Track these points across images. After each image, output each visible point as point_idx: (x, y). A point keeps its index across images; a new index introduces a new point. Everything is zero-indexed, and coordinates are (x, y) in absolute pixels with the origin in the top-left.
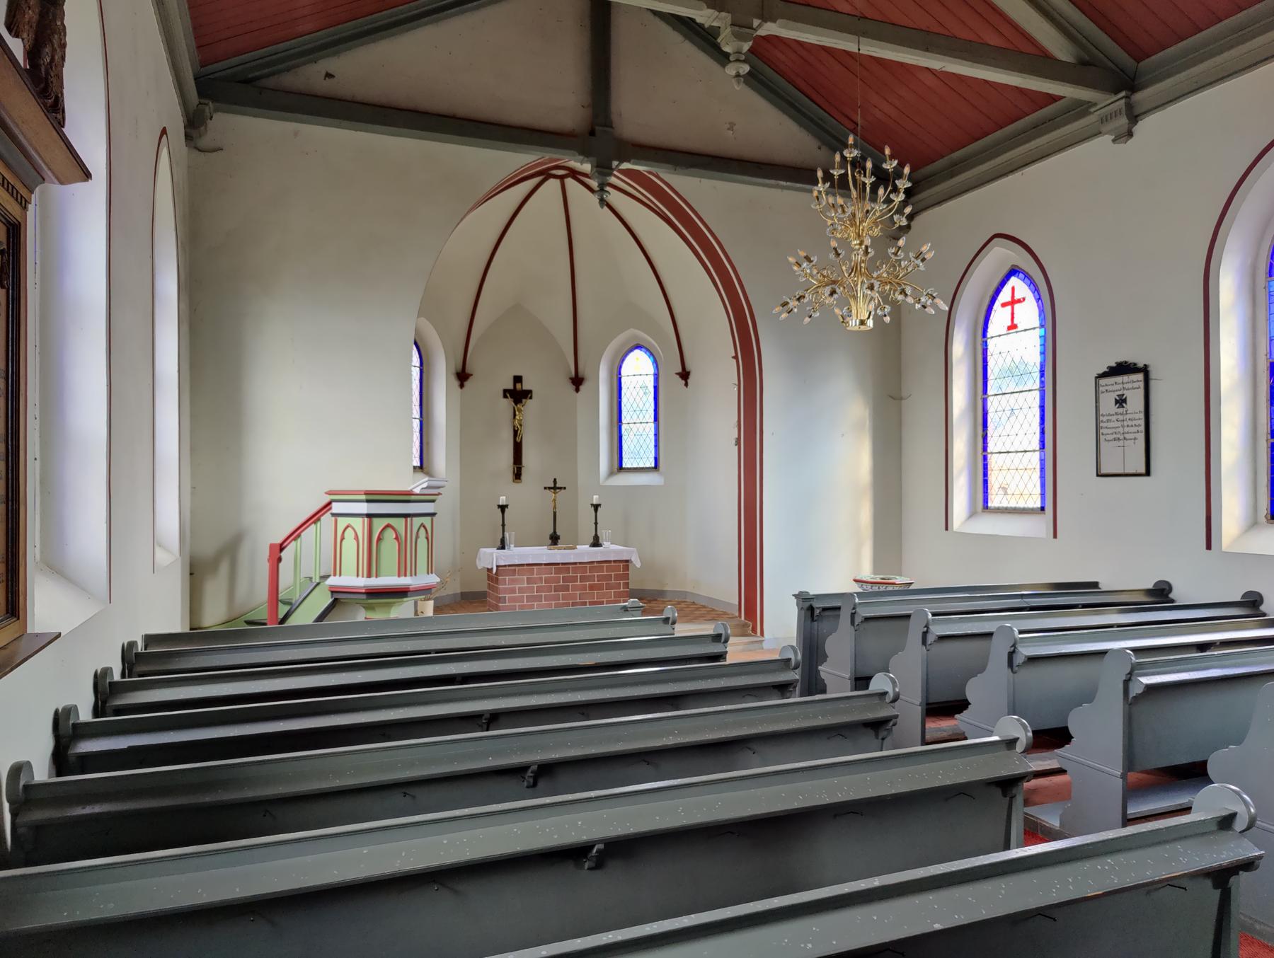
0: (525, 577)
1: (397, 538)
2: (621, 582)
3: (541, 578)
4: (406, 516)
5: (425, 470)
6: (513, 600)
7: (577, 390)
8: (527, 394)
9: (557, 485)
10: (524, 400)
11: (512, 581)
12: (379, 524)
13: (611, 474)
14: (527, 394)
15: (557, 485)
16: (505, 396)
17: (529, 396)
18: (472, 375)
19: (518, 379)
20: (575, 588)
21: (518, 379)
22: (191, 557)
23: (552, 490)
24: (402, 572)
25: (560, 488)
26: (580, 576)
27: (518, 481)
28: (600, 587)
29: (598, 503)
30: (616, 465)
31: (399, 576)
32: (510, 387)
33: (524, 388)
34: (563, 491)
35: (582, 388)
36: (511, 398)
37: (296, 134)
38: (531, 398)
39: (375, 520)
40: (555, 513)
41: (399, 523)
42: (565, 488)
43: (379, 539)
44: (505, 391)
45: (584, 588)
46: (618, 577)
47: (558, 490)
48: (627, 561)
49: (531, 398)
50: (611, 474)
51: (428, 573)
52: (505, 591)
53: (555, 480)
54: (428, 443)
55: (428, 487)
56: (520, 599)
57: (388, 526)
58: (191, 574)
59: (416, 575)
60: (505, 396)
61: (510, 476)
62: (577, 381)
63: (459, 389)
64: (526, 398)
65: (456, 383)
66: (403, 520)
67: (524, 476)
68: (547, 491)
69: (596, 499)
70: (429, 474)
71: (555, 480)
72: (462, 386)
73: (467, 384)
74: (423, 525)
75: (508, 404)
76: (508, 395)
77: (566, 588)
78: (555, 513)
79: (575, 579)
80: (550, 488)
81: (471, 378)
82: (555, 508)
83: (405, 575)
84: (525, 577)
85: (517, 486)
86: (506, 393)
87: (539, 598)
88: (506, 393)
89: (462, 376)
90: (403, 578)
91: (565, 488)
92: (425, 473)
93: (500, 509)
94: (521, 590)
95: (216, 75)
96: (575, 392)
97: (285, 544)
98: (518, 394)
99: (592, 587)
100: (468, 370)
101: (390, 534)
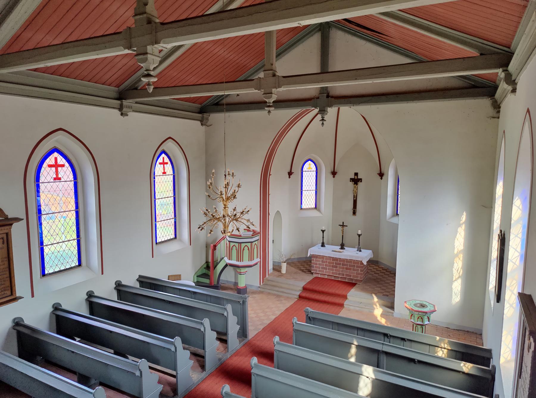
0: (321, 260)
1: (236, 249)
2: (359, 269)
3: (327, 261)
4: (239, 243)
5: (317, 209)
6: (317, 267)
7: (381, 179)
8: (360, 180)
9: (344, 225)
10: (358, 183)
11: (316, 261)
12: (232, 244)
13: (393, 216)
14: (360, 180)
15: (344, 225)
16: (351, 181)
17: (360, 181)
18: (337, 173)
19: (356, 174)
20: (340, 268)
21: (356, 174)
22: (206, 243)
23: (342, 226)
24: (238, 260)
25: (345, 226)
26: (342, 264)
27: (354, 215)
28: (350, 269)
29: (360, 234)
30: (396, 213)
31: (237, 261)
32: (354, 178)
33: (359, 177)
34: (346, 227)
35: (383, 178)
36: (353, 181)
37: (229, 116)
38: (361, 182)
39: (231, 243)
40: (343, 236)
41: (237, 245)
42: (347, 226)
43: (232, 249)
44: (351, 179)
45: (343, 268)
46: (357, 267)
47: (344, 227)
48: (362, 261)
49: (361, 182)
50: (393, 216)
51: (249, 261)
52: (314, 263)
53: (343, 222)
54: (319, 199)
55: (243, 235)
56: (319, 268)
57: (234, 245)
58: (206, 247)
59: (243, 261)
60: (351, 181)
61: (352, 213)
62: (381, 175)
63: (333, 178)
64: (359, 182)
65: (332, 176)
66: (238, 244)
67: (357, 213)
68: (340, 226)
69: (360, 232)
70: (319, 211)
71: (343, 222)
72: (334, 177)
73: (336, 176)
74: (246, 246)
75: (351, 184)
76: (351, 181)
77: (336, 267)
78: (343, 236)
79: (340, 264)
80: (341, 225)
81: (337, 174)
82: (343, 233)
83: (239, 261)
84: (321, 260)
85: (354, 217)
86: (352, 180)
87: (326, 269)
88: (352, 180)
89: (334, 173)
90: (238, 262)
91: (347, 226)
92: (317, 210)
93: (322, 232)
94: (319, 264)
95: (207, 105)
96: (381, 180)
97: (217, 245)
98: (356, 181)
99: (347, 269)
100: (335, 171)
101: (234, 248)
